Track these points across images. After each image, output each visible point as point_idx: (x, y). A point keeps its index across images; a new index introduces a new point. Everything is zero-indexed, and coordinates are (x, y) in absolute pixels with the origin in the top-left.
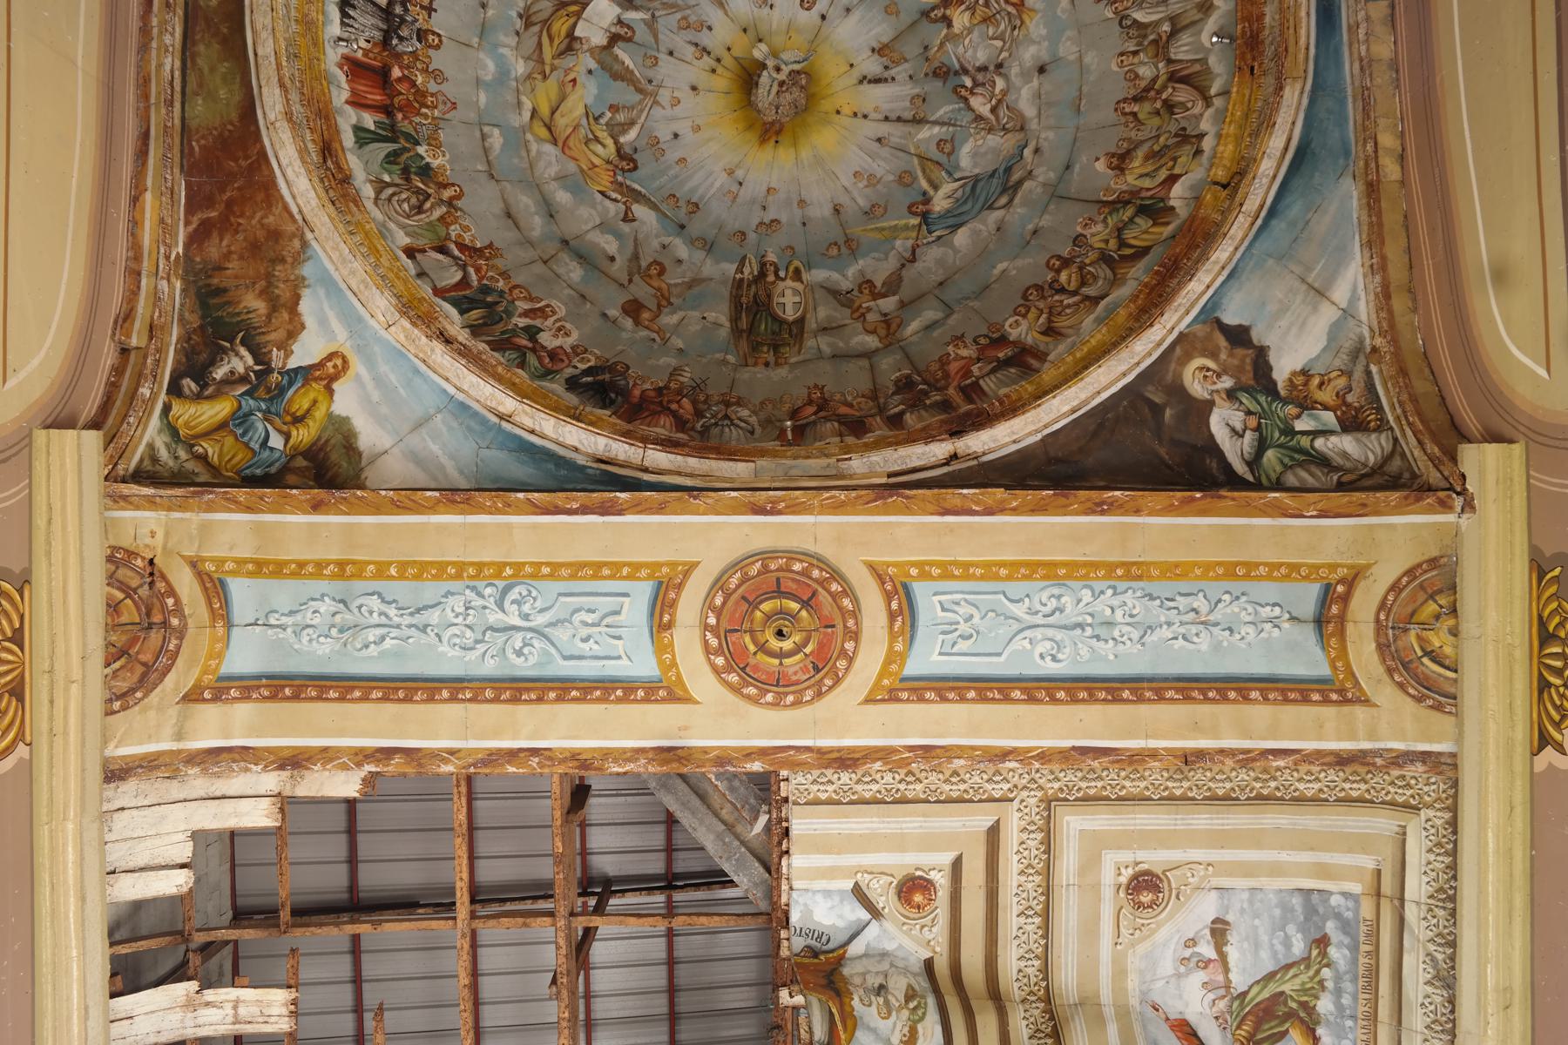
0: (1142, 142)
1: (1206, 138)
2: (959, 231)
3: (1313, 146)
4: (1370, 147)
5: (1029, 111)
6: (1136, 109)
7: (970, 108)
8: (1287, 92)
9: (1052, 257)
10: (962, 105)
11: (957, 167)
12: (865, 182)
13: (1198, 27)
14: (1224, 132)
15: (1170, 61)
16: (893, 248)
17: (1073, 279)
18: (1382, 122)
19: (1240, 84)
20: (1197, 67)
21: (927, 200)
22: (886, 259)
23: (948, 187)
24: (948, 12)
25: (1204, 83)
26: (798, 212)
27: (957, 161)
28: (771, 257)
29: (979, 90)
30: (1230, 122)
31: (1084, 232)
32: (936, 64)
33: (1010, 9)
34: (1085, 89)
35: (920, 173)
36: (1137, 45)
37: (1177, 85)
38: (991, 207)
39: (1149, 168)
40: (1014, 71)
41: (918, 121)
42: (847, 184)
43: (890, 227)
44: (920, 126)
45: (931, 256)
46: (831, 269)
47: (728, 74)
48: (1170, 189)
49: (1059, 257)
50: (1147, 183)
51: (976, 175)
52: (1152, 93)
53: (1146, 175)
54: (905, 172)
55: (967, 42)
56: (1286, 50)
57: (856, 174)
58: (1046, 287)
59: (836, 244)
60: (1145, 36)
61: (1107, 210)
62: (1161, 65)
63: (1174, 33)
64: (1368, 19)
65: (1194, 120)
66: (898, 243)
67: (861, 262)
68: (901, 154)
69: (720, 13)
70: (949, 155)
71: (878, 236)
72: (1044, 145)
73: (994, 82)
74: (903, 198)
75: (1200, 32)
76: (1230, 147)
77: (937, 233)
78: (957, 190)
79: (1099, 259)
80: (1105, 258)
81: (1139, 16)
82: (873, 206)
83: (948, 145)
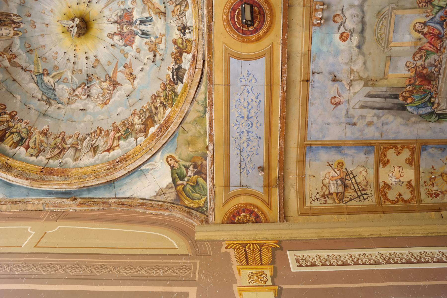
0: (48, 139)
1: (35, 158)
2: (35, 85)
3: (13, 187)
4: (3, 203)
5: (73, 106)
6: (60, 138)
7: (77, 88)
8: (27, 181)
9: (17, 113)
10: (78, 85)
11: (59, 84)
12: (54, 55)
13: (73, 157)
14: (24, 163)
15: (69, 148)
16: (30, 64)
17: (4, 119)
18: (9, 206)
19: (38, 168)
20: (61, 156)
21: (48, 74)
22: (25, 62)
23: (52, 81)
24: (108, 81)
25: (54, 158)
26: (39, 34)
27: (61, 84)
28: (22, 26)
29: (84, 91)
30: (26, 165)
31: (23, 123)
32: (93, 77)
33: (105, 100)
34: (74, 123)
35: (58, 72)
36: (80, 139)
37: (60, 150)
38: (43, 94)
39: (37, 141)
40: (87, 101)
41: (73, 72)
42: (53, 49)
43: (38, 63)
44: (71, 72)
45: (27, 76)
46: (20, 45)
47: (85, 10)
48: (24, 147)
49: (15, 115)
50: (32, 140)
51: (55, 90)
52: (62, 142)
53: (35, 140)
54: (58, 68)
55: (99, 87)
56: (38, 182)
57: (57, 52)
58: (3, 111)
59: (30, 46)
60: (81, 141)
61: (29, 129)
62: (69, 146)
63: (77, 149)
64: (38, 204)
65: (45, 154)
66: (33, 66)
67: (24, 54)
68: (64, 66)
69: (103, 6)
70: (63, 82)
71: (35, 59)
72: (61, 110)
73: (85, 95)
74: (49, 68)
75: (70, 157)
76: (18, 165)
77: (35, 77)
78: (51, 84)
79: (9, 127)
80: (9, 128)
81: (87, 140)
82: (46, 58)
83: (66, 81)
